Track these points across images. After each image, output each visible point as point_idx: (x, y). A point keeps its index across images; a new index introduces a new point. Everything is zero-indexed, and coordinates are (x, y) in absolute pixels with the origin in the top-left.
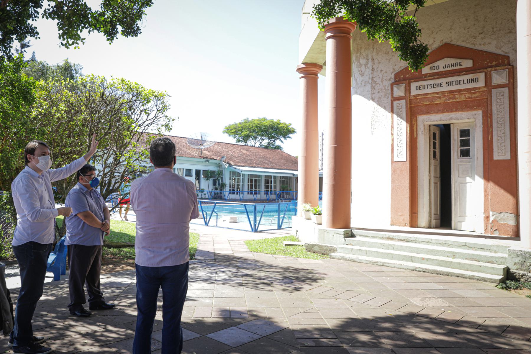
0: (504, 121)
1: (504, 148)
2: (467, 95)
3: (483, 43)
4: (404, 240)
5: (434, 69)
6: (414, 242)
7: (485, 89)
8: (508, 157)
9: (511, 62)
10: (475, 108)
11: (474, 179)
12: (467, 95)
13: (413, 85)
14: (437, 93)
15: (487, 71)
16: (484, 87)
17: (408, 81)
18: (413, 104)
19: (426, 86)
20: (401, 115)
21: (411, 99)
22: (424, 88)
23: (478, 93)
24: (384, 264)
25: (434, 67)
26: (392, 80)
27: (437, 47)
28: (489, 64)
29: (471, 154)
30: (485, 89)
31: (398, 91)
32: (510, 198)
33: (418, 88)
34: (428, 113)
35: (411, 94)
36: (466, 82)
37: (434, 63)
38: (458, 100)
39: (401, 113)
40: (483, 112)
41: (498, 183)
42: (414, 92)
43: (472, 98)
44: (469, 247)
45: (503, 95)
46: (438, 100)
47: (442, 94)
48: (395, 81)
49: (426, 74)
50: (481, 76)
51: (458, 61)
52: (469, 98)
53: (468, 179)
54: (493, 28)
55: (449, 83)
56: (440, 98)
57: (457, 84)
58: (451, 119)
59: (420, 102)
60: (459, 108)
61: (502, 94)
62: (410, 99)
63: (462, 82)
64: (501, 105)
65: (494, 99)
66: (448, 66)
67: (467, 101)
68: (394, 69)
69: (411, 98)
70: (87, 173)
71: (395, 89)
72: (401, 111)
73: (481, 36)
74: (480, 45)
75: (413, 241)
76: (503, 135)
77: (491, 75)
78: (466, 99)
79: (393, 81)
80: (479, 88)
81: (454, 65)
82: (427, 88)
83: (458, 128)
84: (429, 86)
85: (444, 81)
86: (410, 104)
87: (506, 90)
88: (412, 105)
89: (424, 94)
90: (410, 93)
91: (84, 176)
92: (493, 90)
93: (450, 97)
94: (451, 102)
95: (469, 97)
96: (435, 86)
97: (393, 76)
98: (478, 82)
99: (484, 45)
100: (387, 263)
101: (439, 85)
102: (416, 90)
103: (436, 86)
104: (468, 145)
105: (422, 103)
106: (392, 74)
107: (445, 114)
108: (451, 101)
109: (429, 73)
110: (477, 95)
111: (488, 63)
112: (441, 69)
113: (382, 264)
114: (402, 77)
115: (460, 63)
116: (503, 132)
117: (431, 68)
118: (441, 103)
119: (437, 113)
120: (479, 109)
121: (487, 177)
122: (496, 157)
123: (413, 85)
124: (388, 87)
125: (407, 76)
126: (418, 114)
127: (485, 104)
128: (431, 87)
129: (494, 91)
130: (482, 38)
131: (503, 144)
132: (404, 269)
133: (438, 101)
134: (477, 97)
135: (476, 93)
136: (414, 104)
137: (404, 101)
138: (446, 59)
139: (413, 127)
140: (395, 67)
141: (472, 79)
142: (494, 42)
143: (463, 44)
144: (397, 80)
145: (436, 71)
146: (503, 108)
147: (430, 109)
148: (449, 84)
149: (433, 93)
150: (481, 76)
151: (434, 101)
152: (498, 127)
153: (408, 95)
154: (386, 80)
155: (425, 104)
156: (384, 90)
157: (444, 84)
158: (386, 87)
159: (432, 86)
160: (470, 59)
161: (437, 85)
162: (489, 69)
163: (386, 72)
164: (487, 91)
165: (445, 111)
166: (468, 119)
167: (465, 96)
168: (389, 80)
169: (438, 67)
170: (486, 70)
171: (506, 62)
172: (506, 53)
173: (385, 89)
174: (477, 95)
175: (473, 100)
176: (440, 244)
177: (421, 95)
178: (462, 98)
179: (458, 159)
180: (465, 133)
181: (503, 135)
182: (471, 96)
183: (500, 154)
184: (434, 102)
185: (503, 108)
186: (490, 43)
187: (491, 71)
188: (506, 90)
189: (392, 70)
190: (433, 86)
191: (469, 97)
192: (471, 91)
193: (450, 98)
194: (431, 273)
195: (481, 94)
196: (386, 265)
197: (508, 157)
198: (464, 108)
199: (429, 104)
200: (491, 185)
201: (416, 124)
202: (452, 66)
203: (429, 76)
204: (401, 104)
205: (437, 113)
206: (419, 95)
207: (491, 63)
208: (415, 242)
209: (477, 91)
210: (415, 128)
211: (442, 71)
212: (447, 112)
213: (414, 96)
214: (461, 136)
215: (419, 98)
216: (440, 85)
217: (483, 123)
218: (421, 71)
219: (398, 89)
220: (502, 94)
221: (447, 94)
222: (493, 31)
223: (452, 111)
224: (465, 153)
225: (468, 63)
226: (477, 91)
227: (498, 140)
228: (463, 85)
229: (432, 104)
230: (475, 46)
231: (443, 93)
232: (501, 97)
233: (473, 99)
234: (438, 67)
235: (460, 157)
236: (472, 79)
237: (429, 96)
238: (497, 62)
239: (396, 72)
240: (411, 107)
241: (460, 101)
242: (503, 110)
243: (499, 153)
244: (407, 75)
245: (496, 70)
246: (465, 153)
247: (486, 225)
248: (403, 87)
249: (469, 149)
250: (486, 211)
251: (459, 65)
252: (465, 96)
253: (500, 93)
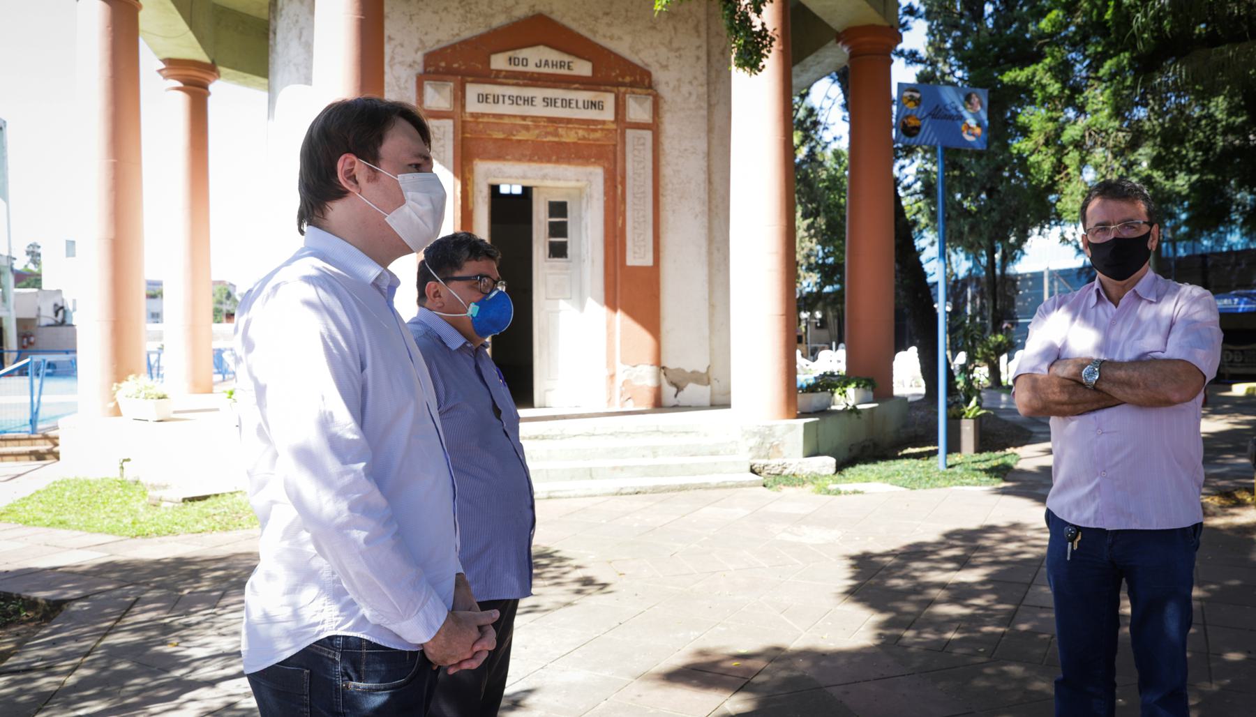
0: (644, 192)
1: (643, 243)
2: (581, 133)
3: (609, 34)
4: (536, 438)
5: (517, 63)
6: (559, 437)
7: (613, 126)
8: (648, 261)
9: (653, 84)
10: (593, 160)
11: (582, 306)
12: (581, 133)
13: (472, 91)
14: (524, 118)
15: (618, 91)
16: (613, 122)
17: (459, 77)
18: (468, 133)
19: (501, 99)
20: (442, 154)
22: (496, 100)
23: (600, 132)
24: (552, 494)
25: (517, 60)
26: (416, 66)
27: (522, 17)
28: (620, 79)
29: (569, 252)
30: (613, 126)
31: (437, 96)
32: (646, 338)
33: (483, 98)
34: (499, 157)
36: (581, 104)
37: (518, 51)
38: (564, 140)
39: (442, 149)
40: (606, 171)
41: (632, 313)
42: (473, 106)
43: (589, 140)
44: (663, 432)
45: (644, 144)
46: (524, 132)
47: (532, 121)
48: (425, 72)
49: (499, 72)
50: (609, 99)
51: (566, 58)
52: (584, 138)
53: (563, 304)
54: (627, 11)
55: (549, 101)
56: (527, 128)
57: (564, 105)
58: (544, 177)
60: (564, 155)
61: (642, 141)
63: (573, 105)
64: (641, 162)
65: (629, 148)
66: (545, 65)
67: (579, 144)
68: (421, 41)
69: (464, 119)
70: (458, 266)
71: (429, 90)
72: (443, 146)
73: (606, 19)
74: (604, 36)
75: (557, 436)
76: (642, 219)
77: (624, 101)
78: (579, 139)
79: (419, 68)
80: (604, 122)
81: (556, 65)
82: (504, 102)
83: (545, 199)
84: (506, 99)
85: (539, 93)
86: (463, 133)
87: (648, 135)
88: (468, 135)
89: (495, 116)
90: (463, 106)
91: (447, 280)
92: (630, 133)
93: (548, 130)
94: (549, 142)
95: (584, 136)
96: (519, 102)
97: (419, 57)
98: (602, 109)
99: (612, 38)
100: (558, 491)
101: (528, 101)
102: (479, 101)
103: (521, 102)
104: (565, 235)
105: (489, 135)
106: (416, 52)
107: (534, 166)
108: (550, 138)
109: (507, 71)
110: (598, 135)
111: (617, 76)
112: (531, 68)
113: (545, 495)
114: (443, 64)
115: (569, 63)
116: (641, 213)
117: (510, 59)
118: (527, 141)
119: (519, 160)
120: (599, 165)
121: (612, 302)
122: (631, 261)
123: (472, 91)
124: (406, 81)
125: (456, 65)
127: (611, 156)
128: (511, 102)
129: (630, 133)
130: (609, 25)
131: (642, 237)
132: (595, 496)
133: (523, 136)
134: (598, 140)
135: (595, 130)
136: (471, 134)
138: (541, 48)
140: (425, 38)
141: (592, 102)
142: (628, 39)
143: (574, 26)
144: (431, 69)
145: (520, 68)
146: (644, 168)
147: (505, 149)
148: (549, 102)
149: (515, 116)
150: (609, 99)
151: (515, 133)
152: (634, 204)
154: (402, 63)
155: (495, 136)
156: (396, 88)
157: (538, 101)
158: (403, 81)
159: (515, 100)
160: (588, 60)
161: (525, 100)
162: (622, 89)
163: (402, 45)
164: (616, 130)
165: (536, 158)
166: (578, 180)
167: (577, 133)
168: (410, 66)
169: (525, 61)
170: (615, 89)
171: (646, 82)
172: (647, 65)
173: (399, 86)
174: (598, 135)
175: (590, 144)
176: (611, 434)
177: (488, 115)
178: (569, 136)
179: (546, 261)
180: (558, 209)
181: (642, 219)
182: (589, 134)
183: (636, 255)
184: (514, 135)
185: (644, 168)
186: (620, 38)
187: (625, 93)
188: (648, 135)
189: (416, 43)
190: (515, 99)
191: (584, 136)
192: (588, 125)
193: (547, 134)
194: (651, 493)
195: (606, 135)
196: (557, 494)
197: (648, 261)
198: (573, 159)
199: (503, 139)
200: (620, 316)
202: (553, 65)
203: (505, 77)
204: (442, 129)
205: (519, 159)
206: (483, 115)
207: (623, 78)
208: (561, 439)
209: (599, 127)
210: (469, 188)
211: (533, 73)
212: (540, 160)
213: (472, 115)
214: (551, 215)
215: (482, 122)
216: (529, 101)
217: (606, 193)
218: (489, 63)
219: (437, 90)
220: (642, 141)
221: (542, 124)
222: (627, 16)
223: (549, 161)
224: (558, 251)
225: (583, 68)
226: (599, 127)
227: (635, 228)
228: (576, 110)
229: (509, 140)
230: (595, 36)
232: (641, 147)
233: (592, 142)
234: (525, 61)
235: (550, 257)
236: (592, 102)
237: (506, 121)
238: (632, 79)
239: (428, 50)
240: (463, 139)
241: (566, 143)
242: (642, 171)
243: (635, 253)
244: (455, 63)
245: (634, 93)
246: (558, 251)
247: (611, 391)
248: (448, 88)
249: (566, 242)
250: (610, 363)
251: (566, 67)
252: (577, 133)
253: (639, 139)
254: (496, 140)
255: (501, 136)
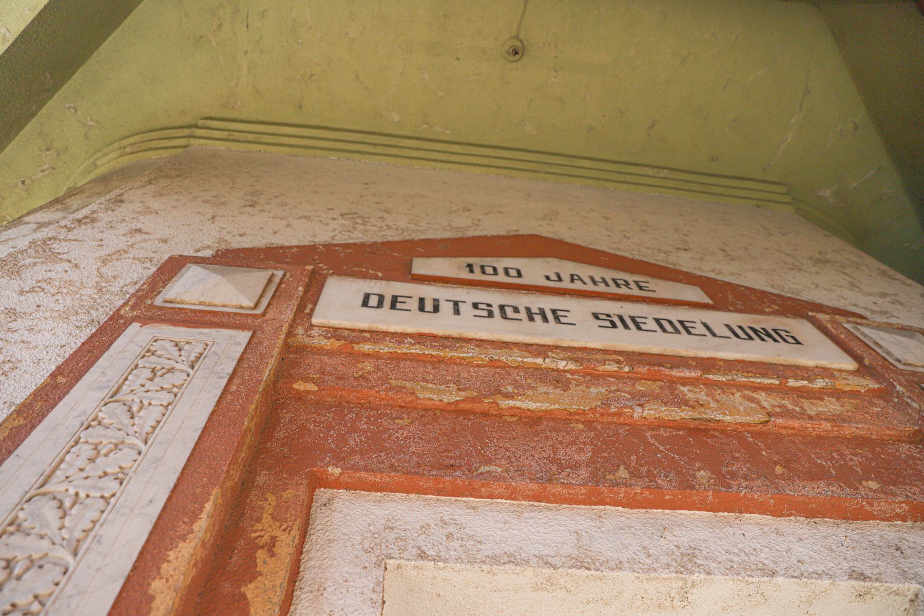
18: (306, 379)
21: (302, 349)
35: (315, 320)
47: (576, 360)
56: (558, 379)
59: (385, 379)
62: (287, 347)
88: (300, 386)
126: (339, 458)
137: (243, 337)
139: (250, 573)
153: (288, 315)
184: (508, 396)
201: (285, 547)
206: (377, 335)
213: (335, 332)
231: (579, 355)
237: (470, 353)
254: (431, 413)
255: (451, 396)
